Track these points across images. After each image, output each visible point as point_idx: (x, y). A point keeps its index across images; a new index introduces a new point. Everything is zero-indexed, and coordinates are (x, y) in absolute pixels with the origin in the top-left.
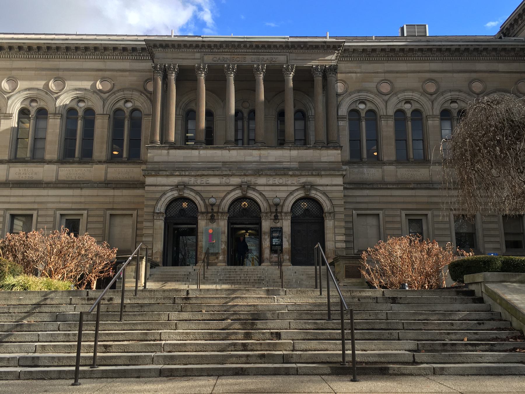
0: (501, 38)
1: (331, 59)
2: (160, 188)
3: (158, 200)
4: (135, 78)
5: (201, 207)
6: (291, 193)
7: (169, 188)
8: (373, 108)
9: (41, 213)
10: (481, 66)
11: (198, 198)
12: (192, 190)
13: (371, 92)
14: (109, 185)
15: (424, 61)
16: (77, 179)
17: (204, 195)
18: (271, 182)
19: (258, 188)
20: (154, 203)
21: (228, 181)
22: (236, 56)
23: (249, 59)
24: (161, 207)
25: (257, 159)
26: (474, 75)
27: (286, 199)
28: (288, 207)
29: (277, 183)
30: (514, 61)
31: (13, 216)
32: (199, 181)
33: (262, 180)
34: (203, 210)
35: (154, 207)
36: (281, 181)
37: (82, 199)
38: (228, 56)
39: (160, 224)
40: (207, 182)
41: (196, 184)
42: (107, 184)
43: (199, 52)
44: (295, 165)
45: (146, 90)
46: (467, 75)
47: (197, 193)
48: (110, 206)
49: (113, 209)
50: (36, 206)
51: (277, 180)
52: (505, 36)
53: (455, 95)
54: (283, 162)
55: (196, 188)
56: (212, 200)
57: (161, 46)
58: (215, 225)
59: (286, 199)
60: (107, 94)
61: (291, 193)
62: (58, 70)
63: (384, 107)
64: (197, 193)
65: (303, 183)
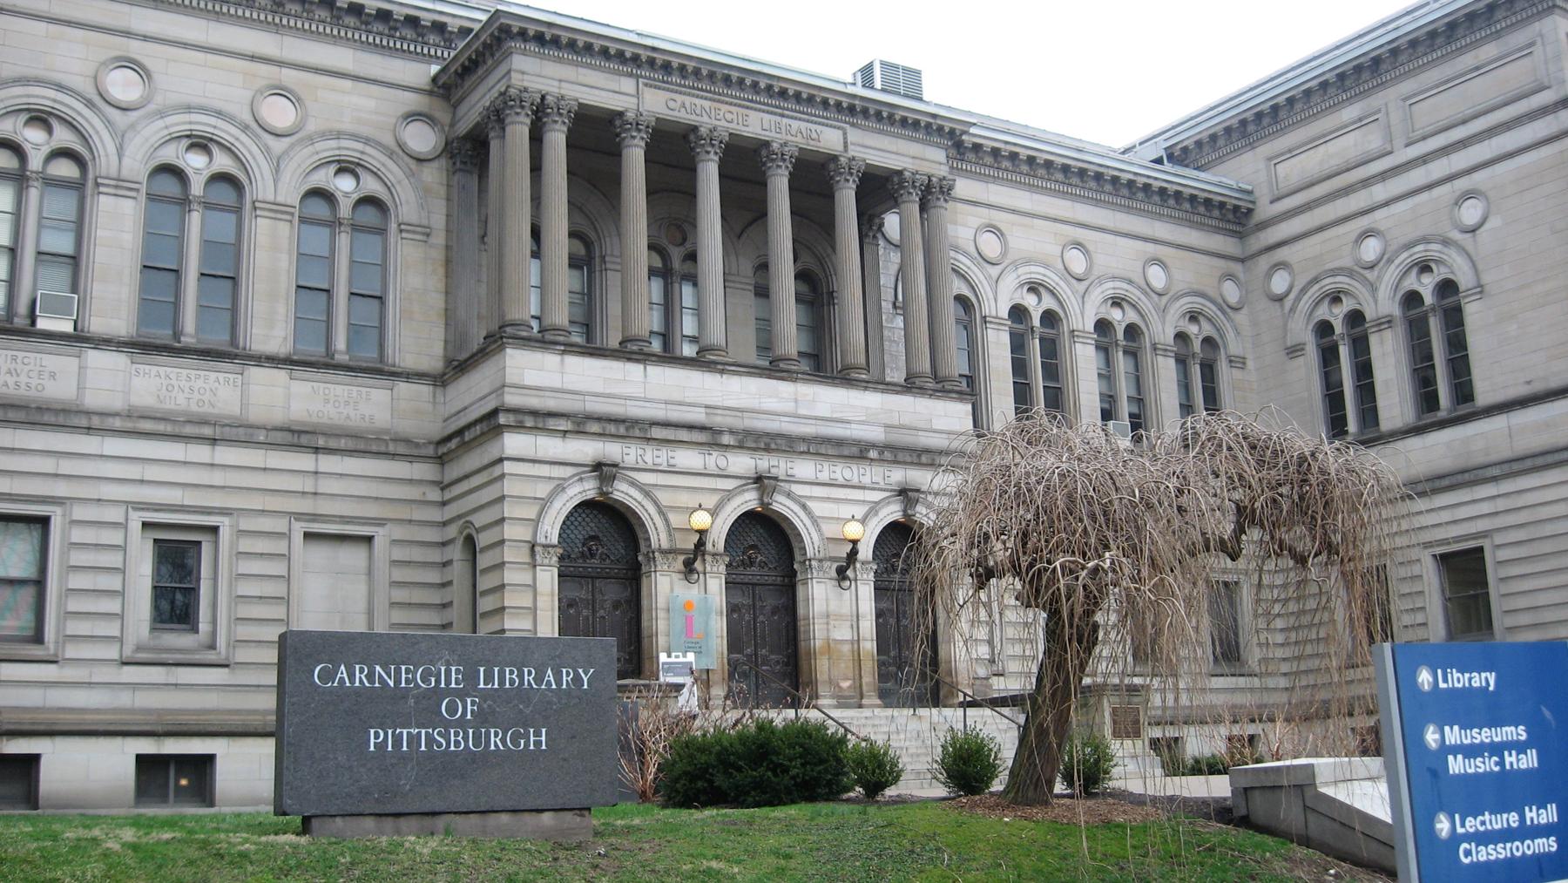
0: (1159, 161)
1: (928, 159)
2: (545, 470)
3: (544, 504)
4: (371, 104)
5: (658, 536)
7: (570, 471)
8: (966, 292)
9: (80, 512)
10: (1162, 229)
11: (652, 509)
12: (633, 484)
14: (304, 440)
15: (1064, 195)
16: (194, 408)
17: (665, 498)
18: (824, 476)
19: (798, 490)
20: (531, 512)
21: (722, 462)
22: (725, 108)
24: (551, 530)
25: (789, 407)
26: (1151, 248)
29: (841, 481)
32: (651, 455)
33: (804, 468)
34: (665, 545)
35: (536, 522)
36: (847, 474)
37: (217, 478)
38: (707, 104)
39: (548, 579)
40: (672, 462)
41: (641, 465)
42: (299, 437)
43: (631, 75)
44: (876, 434)
45: (401, 146)
46: (1139, 244)
48: (305, 506)
49: (315, 517)
50: (61, 489)
52: (1171, 157)
54: (848, 422)
57: (540, 39)
60: (287, 141)
62: (127, 34)
63: (991, 296)
64: (646, 491)
65: (899, 483)
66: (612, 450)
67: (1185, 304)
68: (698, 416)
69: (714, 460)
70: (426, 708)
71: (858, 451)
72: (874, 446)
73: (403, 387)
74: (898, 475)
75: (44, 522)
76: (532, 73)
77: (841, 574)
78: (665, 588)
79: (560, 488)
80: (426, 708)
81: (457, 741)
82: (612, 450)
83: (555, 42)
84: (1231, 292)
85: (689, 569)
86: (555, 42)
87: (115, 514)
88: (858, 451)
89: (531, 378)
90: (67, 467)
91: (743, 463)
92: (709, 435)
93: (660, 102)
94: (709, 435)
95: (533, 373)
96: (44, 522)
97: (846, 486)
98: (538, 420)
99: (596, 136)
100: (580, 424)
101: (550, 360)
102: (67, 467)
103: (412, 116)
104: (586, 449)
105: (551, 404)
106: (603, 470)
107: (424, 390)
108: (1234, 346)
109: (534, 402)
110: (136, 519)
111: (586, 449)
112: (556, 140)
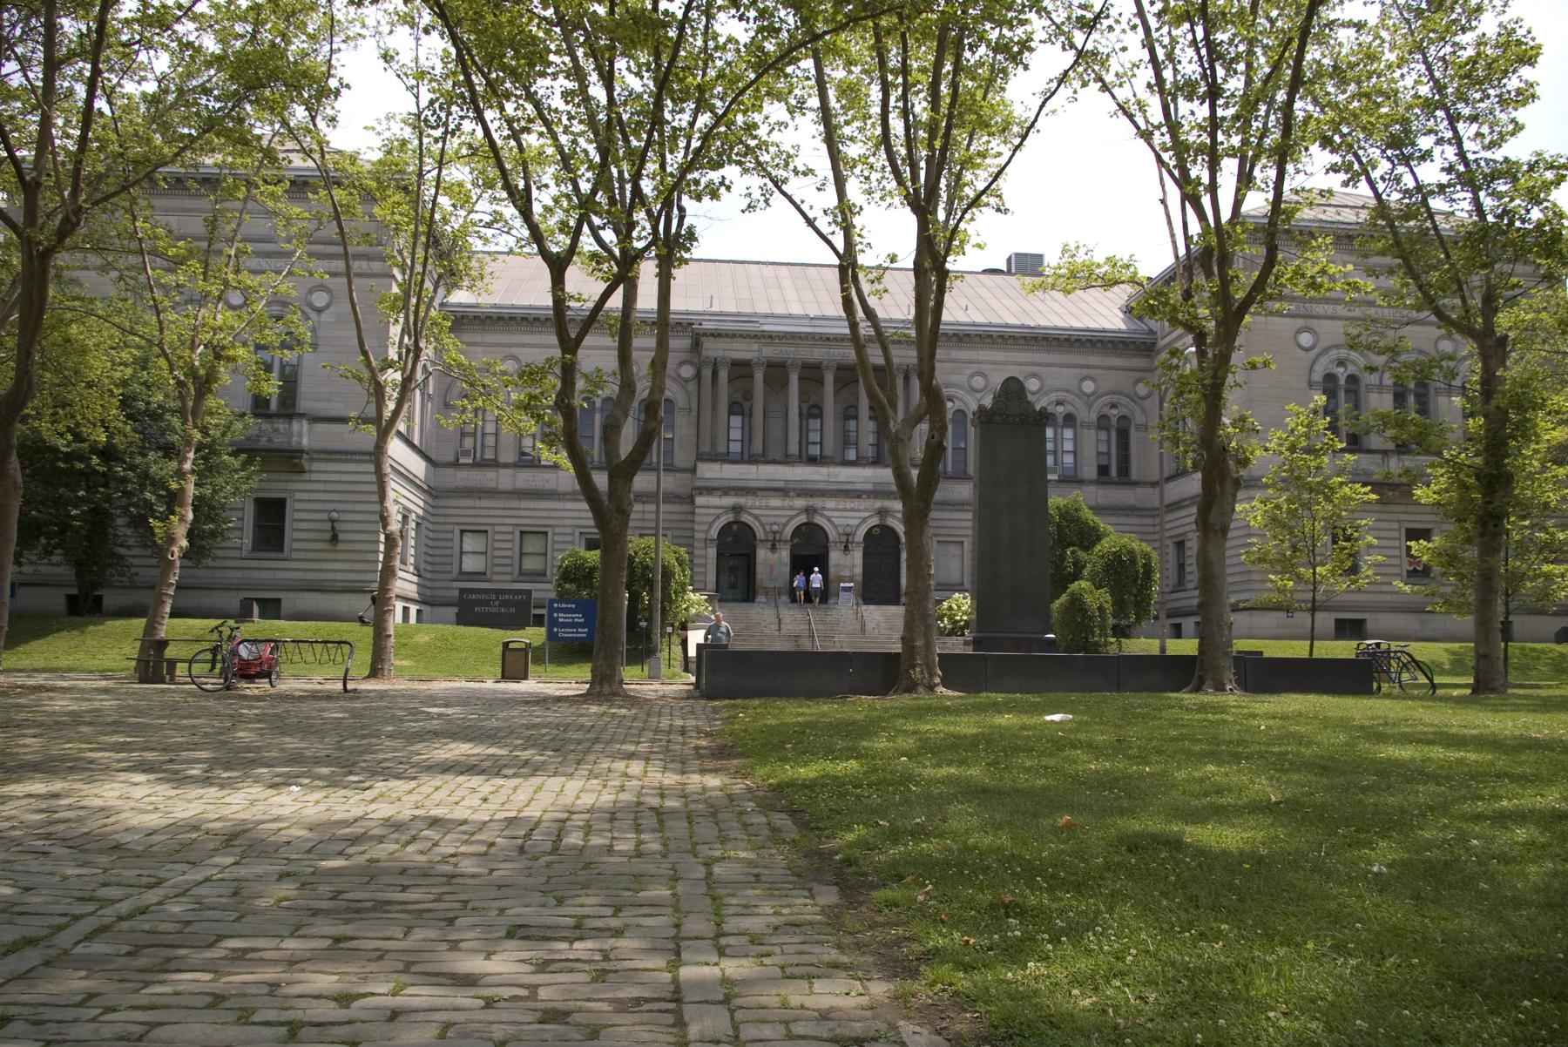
2: (712, 511)
3: (711, 524)
5: (760, 534)
6: (865, 520)
9: (557, 530)
10: (1094, 360)
13: (961, 388)
17: (764, 520)
20: (705, 527)
23: (816, 354)
24: (714, 533)
26: (1085, 372)
27: (858, 526)
28: (860, 535)
30: (1134, 356)
31: (522, 533)
33: (831, 503)
35: (707, 532)
39: (712, 552)
44: (869, 487)
46: (1077, 371)
47: (756, 517)
50: (551, 522)
51: (849, 504)
53: (1061, 395)
55: (756, 512)
56: (775, 528)
58: (776, 556)
59: (858, 526)
61: (865, 520)
64: (756, 517)
66: (742, 500)
67: (1107, 399)
68: (781, 485)
69: (787, 502)
70: (487, 603)
71: (858, 494)
72: (863, 492)
73: (679, 475)
74: (878, 504)
75: (546, 533)
76: (712, 349)
77: (846, 548)
78: (762, 554)
79: (718, 517)
80: (487, 603)
81: (494, 610)
82: (742, 500)
83: (719, 335)
84: (1142, 389)
85: (773, 548)
86: (719, 335)
87: (569, 530)
88: (858, 494)
89: (707, 475)
90: (553, 514)
91: (801, 503)
92: (783, 492)
93: (769, 352)
94: (783, 492)
95: (710, 472)
96: (546, 533)
97: (852, 510)
98: (709, 491)
99: (741, 369)
100: (726, 491)
101: (716, 466)
102: (553, 514)
103: (682, 363)
104: (729, 501)
105: (715, 484)
106: (737, 509)
107: (688, 475)
108: (1139, 419)
109: (708, 484)
110: (577, 531)
111: (729, 501)
112: (723, 374)
